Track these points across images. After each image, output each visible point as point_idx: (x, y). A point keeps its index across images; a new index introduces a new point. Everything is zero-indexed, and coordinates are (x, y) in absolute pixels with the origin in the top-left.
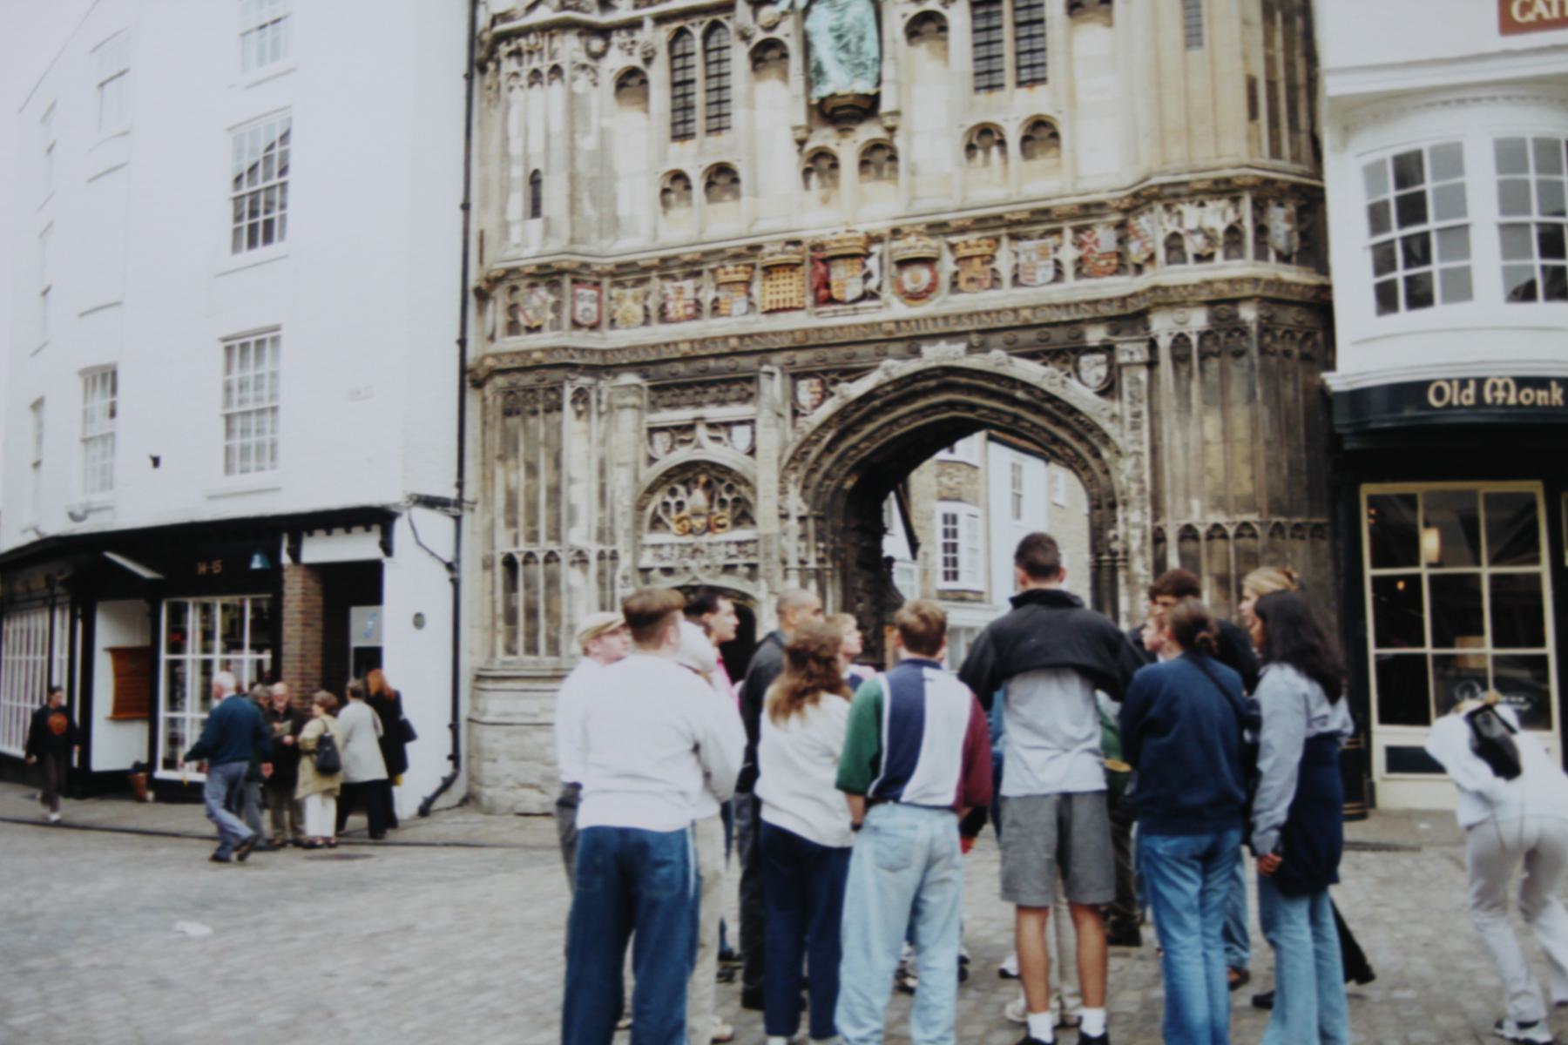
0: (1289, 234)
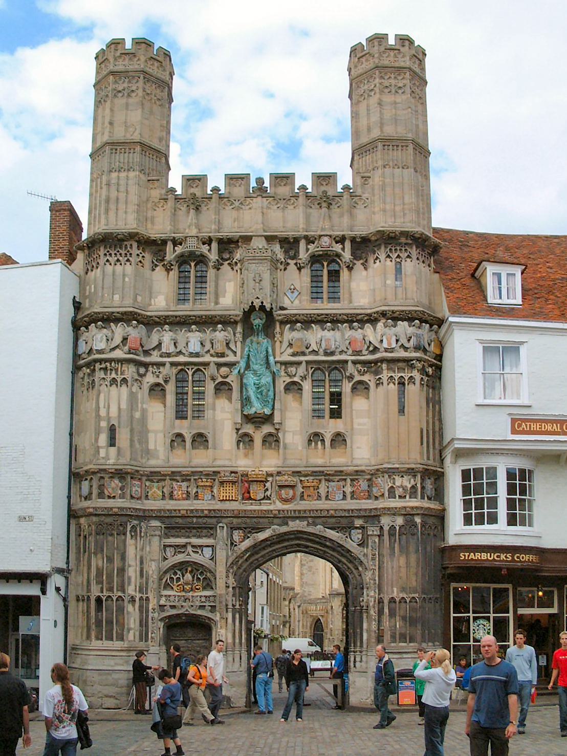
0: (432, 489)
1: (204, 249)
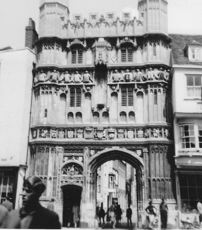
1: (82, 43)
